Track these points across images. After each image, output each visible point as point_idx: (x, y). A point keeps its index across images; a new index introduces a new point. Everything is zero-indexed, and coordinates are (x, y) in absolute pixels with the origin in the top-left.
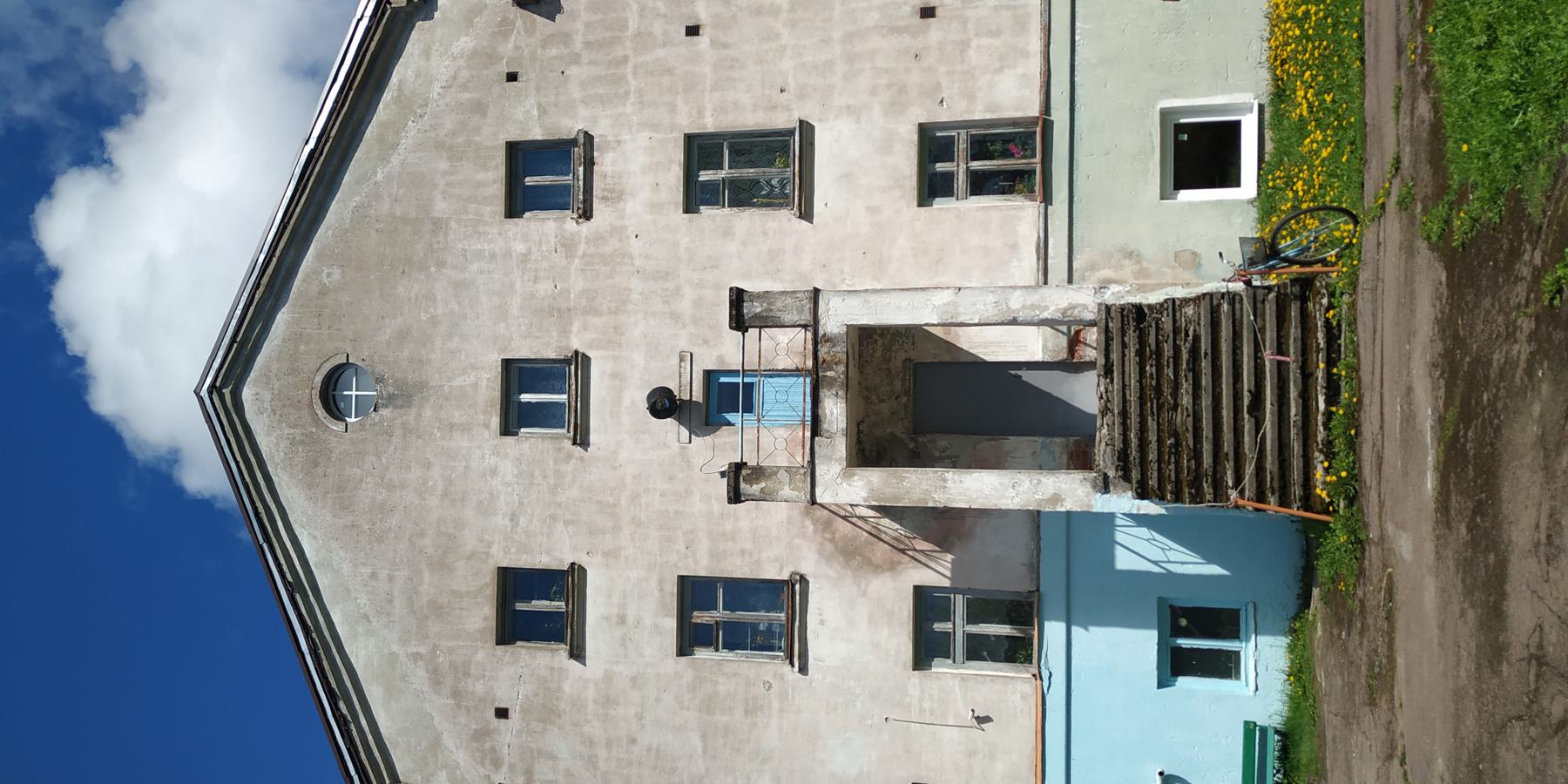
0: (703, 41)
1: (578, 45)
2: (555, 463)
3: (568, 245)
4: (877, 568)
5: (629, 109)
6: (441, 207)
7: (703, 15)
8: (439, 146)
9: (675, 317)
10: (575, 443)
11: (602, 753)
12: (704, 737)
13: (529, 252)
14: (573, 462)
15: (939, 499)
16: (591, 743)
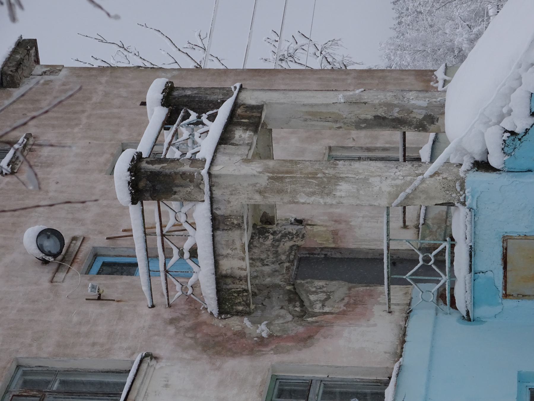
5: (76, 130)
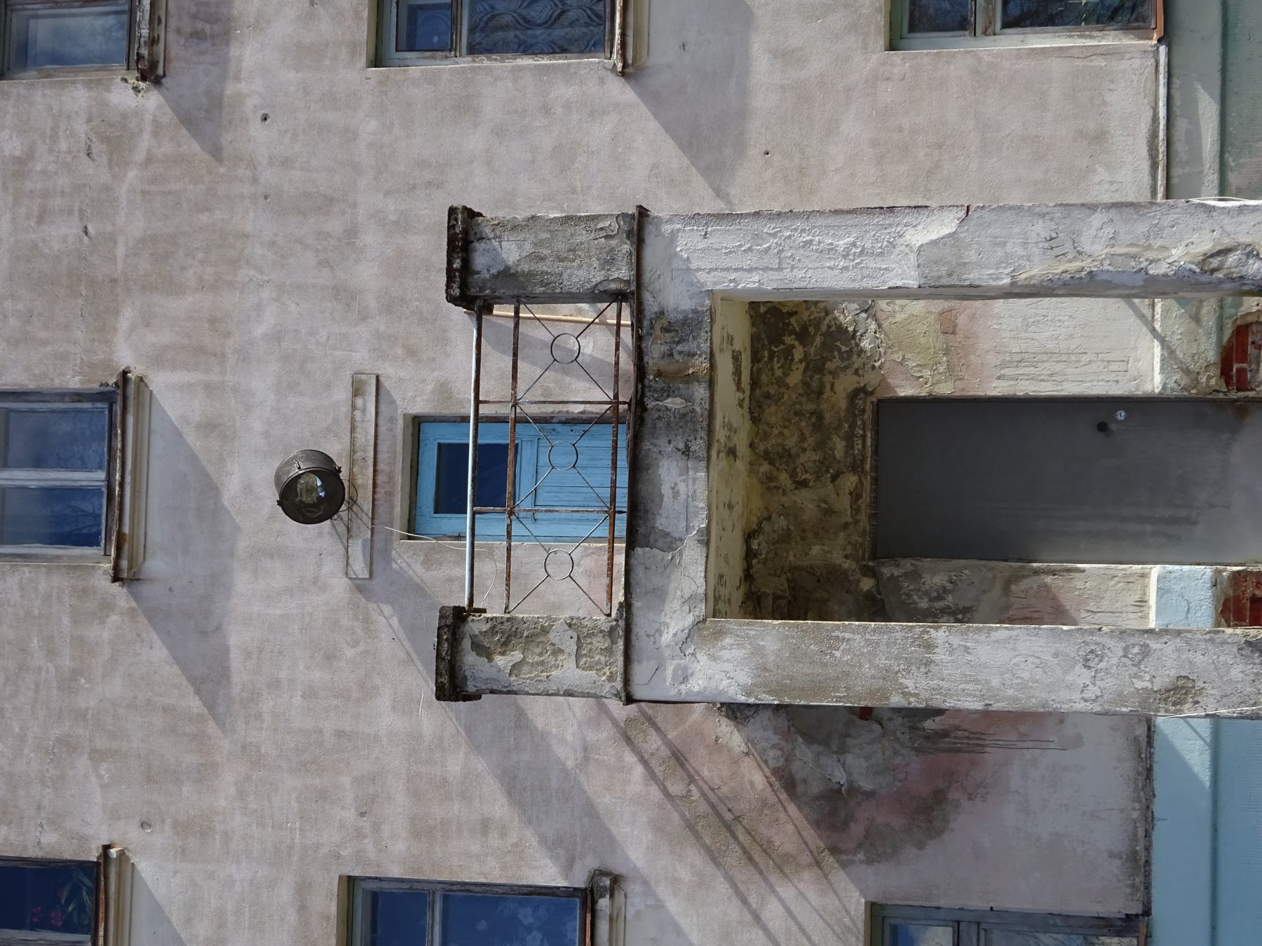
2: (75, 621)
3: (114, 137)
9: (344, 295)
10: (116, 579)
13: (30, 155)
14: (114, 618)
15: (915, 688)
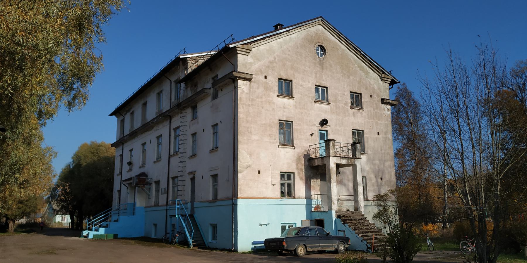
0: (377, 135)
1: (376, 111)
4: (297, 165)
6: (351, 78)
7: (381, 136)
8: (361, 79)
11: (260, 100)
12: (264, 124)
15: (332, 181)
16: (261, 98)
